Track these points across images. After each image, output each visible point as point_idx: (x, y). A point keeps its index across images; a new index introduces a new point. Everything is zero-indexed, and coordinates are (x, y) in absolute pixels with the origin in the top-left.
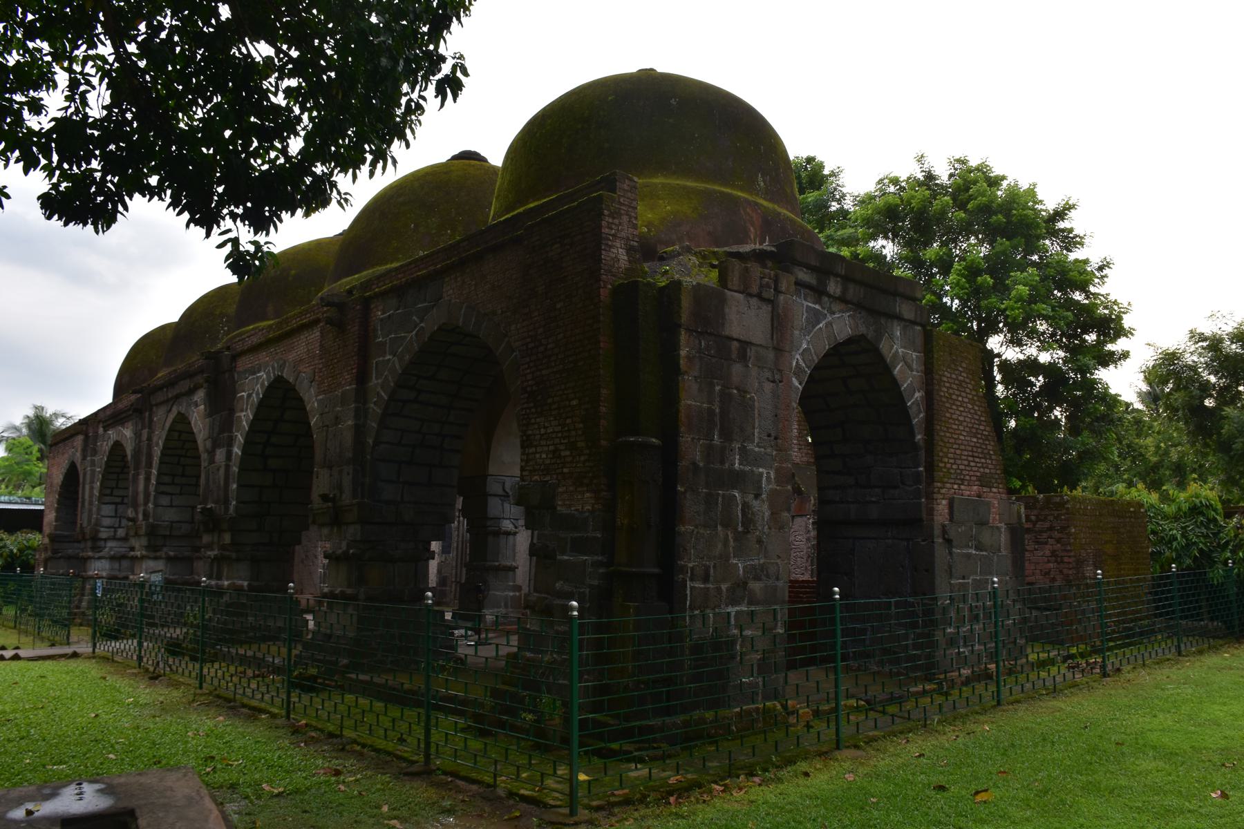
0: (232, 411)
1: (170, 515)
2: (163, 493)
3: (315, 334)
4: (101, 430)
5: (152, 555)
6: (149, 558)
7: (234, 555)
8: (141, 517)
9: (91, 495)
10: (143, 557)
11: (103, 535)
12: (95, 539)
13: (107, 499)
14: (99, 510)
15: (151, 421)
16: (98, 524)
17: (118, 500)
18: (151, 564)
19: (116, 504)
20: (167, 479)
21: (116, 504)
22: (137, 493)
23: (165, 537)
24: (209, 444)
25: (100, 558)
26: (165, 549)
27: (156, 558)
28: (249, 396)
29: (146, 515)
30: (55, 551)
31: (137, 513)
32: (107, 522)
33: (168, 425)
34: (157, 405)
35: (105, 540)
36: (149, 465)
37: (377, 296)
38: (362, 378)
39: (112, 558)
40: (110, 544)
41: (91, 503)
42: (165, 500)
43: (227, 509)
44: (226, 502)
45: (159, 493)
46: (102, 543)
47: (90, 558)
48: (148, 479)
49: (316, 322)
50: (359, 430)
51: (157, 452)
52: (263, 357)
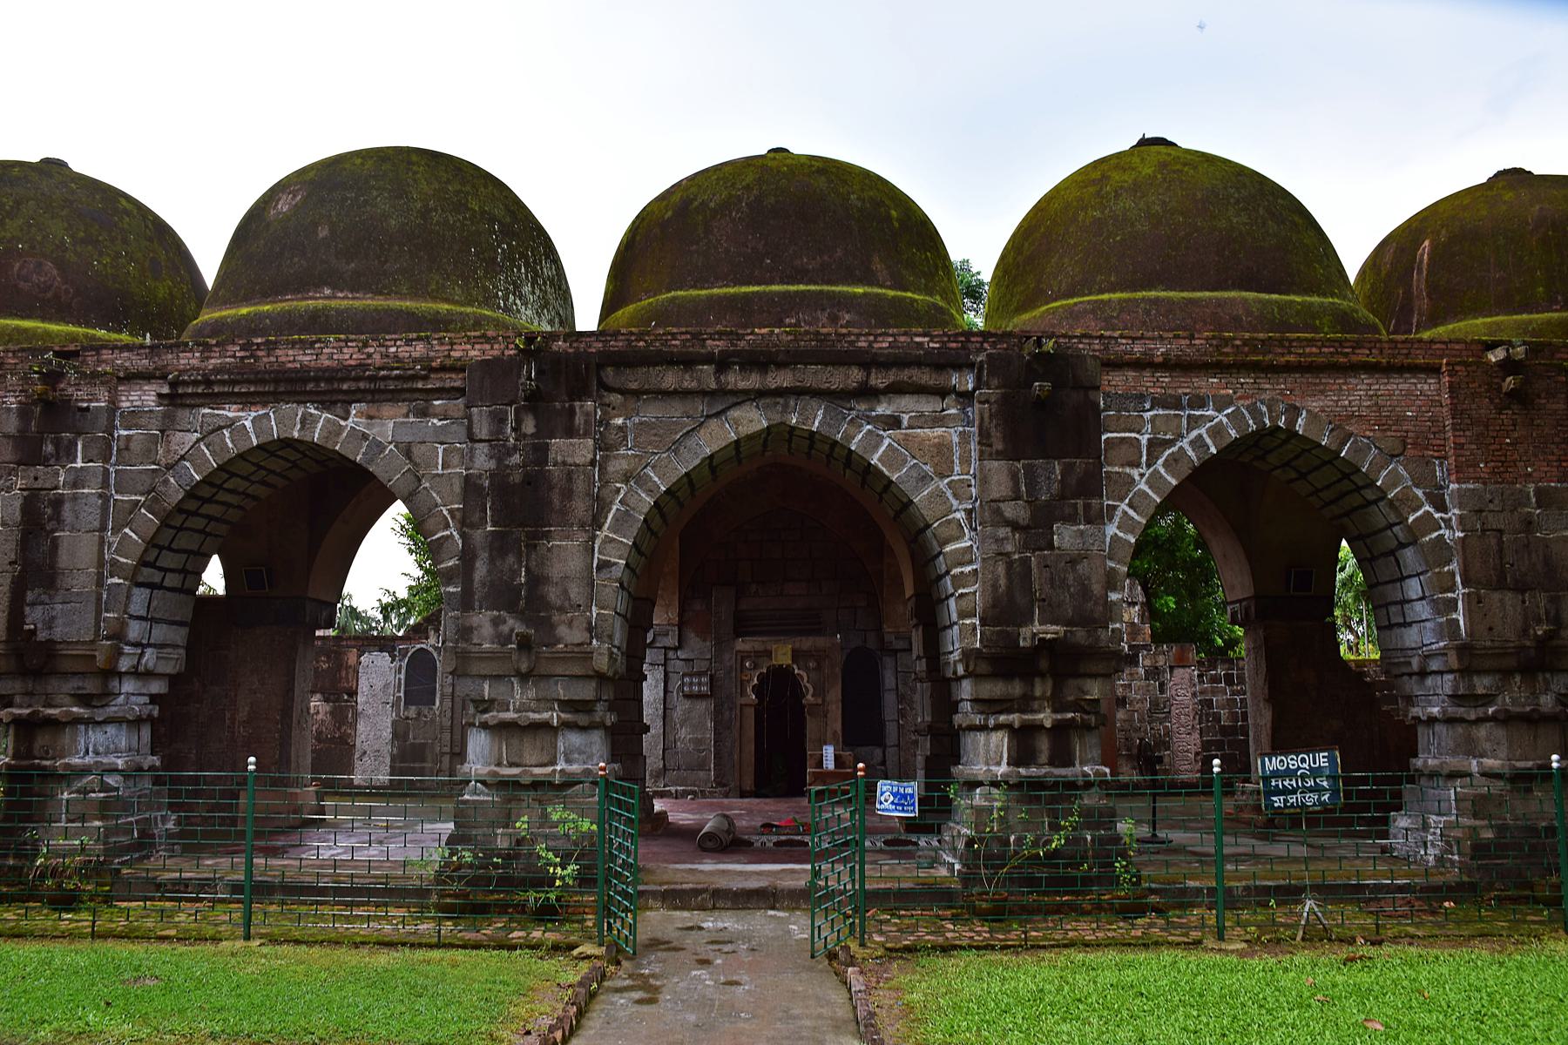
3: (1428, 386)
4: (145, 397)
5: (582, 719)
10: (566, 725)
13: (147, 574)
16: (118, 636)
18: (575, 739)
25: (106, 722)
28: (1156, 446)
47: (77, 721)
49: (1434, 370)
52: (1210, 384)
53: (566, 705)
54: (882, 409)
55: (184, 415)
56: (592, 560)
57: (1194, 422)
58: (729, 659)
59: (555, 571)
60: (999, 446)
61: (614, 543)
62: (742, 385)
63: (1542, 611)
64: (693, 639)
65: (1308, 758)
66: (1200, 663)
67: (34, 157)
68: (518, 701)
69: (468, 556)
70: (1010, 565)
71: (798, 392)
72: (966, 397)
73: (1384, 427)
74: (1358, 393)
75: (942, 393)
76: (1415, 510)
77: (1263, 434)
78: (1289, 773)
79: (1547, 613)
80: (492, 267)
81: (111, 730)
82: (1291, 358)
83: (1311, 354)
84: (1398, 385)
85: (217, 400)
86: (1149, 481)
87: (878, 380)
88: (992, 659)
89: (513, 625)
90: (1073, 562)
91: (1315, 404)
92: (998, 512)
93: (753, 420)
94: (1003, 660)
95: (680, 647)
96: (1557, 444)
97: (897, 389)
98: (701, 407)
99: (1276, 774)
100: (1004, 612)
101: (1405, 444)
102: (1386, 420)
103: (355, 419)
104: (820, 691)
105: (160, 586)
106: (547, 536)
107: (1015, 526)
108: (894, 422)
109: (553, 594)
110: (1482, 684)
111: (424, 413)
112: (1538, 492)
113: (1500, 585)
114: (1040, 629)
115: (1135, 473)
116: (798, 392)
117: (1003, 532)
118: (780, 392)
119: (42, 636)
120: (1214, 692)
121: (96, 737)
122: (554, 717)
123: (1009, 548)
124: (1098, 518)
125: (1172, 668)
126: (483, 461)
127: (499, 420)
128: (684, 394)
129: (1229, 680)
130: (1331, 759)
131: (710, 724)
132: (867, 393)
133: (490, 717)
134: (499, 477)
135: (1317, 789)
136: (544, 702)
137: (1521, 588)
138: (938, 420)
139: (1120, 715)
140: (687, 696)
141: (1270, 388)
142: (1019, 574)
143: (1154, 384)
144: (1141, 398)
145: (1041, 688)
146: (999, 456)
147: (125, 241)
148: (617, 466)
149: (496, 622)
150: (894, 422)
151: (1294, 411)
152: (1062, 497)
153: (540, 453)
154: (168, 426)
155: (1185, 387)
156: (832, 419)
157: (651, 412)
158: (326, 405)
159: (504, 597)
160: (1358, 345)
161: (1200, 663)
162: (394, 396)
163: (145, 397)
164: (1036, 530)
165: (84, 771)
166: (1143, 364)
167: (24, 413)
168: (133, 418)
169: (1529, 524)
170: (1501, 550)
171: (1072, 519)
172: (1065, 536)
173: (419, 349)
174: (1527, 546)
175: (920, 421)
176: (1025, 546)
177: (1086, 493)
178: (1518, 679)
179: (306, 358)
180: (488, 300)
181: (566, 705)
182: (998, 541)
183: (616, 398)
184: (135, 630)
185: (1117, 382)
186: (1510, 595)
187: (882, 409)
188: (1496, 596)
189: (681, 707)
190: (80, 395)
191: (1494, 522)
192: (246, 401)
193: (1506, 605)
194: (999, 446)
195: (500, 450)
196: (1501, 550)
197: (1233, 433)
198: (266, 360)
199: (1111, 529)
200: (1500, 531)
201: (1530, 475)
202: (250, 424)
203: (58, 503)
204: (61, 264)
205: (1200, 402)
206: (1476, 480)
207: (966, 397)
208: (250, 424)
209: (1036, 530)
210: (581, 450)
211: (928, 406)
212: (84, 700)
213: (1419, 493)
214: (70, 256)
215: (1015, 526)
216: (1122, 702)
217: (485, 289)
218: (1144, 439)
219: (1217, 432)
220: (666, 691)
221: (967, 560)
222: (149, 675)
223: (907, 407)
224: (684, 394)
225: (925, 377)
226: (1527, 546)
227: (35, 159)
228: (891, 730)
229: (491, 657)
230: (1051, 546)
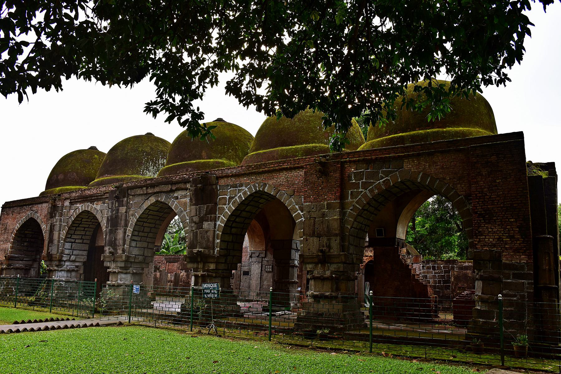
0: (216, 204)
1: (135, 252)
2: (134, 240)
4: (67, 203)
5: (125, 271)
6: (122, 273)
7: (214, 275)
8: (120, 252)
9: (59, 237)
10: (119, 272)
11: (64, 259)
12: (60, 260)
13: (68, 240)
14: (64, 245)
15: (128, 203)
16: (62, 253)
17: (73, 241)
18: (123, 276)
19: (72, 242)
20: (136, 233)
21: (72, 242)
22: (116, 239)
23: (131, 262)
24: (196, 219)
25: (61, 271)
26: (131, 269)
27: (126, 273)
28: (231, 198)
29: (124, 251)
30: (9, 265)
31: (116, 249)
32: (67, 252)
33: (145, 206)
34: (133, 196)
35: (65, 261)
36: (126, 225)
37: (350, 162)
38: (342, 197)
39: (68, 271)
40: (67, 263)
41: (59, 241)
42: (134, 244)
43: (214, 252)
44: (214, 249)
45: (132, 240)
46: (63, 263)
47: (55, 270)
48: (125, 233)
49: (302, 167)
50: (342, 221)
51: (133, 221)
52: (244, 180)
53: (121, 268)
54: (176, 195)
57: (240, 191)
59: (118, 238)
60: (194, 202)
62: (150, 192)
63: (325, 244)
64: (268, 253)
65: (213, 285)
66: (423, 262)
67: (86, 147)
70: (193, 233)
71: (161, 192)
73: (289, 187)
74: (282, 178)
76: (295, 212)
77: (256, 192)
78: (208, 288)
79: (326, 244)
80: (141, 164)
81: (63, 272)
82: (266, 169)
83: (272, 167)
84: (294, 173)
86: (228, 209)
88: (189, 257)
89: (111, 250)
91: (271, 182)
92: (192, 220)
93: (153, 200)
95: (265, 257)
96: (335, 188)
97: (178, 190)
98: (144, 197)
99: (206, 289)
101: (294, 192)
102: (290, 184)
105: (75, 242)
106: (117, 229)
107: (195, 223)
109: (117, 243)
110: (309, 267)
111: (104, 203)
112: (327, 204)
113: (313, 235)
115: (225, 207)
116: (161, 192)
117: (193, 224)
118: (157, 193)
120: (428, 273)
121: (60, 274)
123: (194, 229)
125: (412, 264)
126: (110, 214)
128: (142, 195)
129: (434, 268)
130: (218, 285)
132: (172, 191)
134: (111, 216)
135: (214, 293)
136: (117, 267)
137: (319, 236)
140: (266, 272)
141: (260, 178)
142: (195, 235)
143: (230, 181)
144: (228, 185)
145: (201, 266)
146: (195, 205)
147: (92, 165)
148: (131, 212)
149: (109, 249)
150: (177, 198)
151: (265, 185)
152: (206, 215)
155: (237, 181)
156: (167, 198)
157: (137, 200)
158: (91, 203)
160: (284, 162)
161: (423, 262)
164: (199, 225)
165: (56, 281)
166: (227, 176)
169: (324, 215)
170: (314, 224)
171: (207, 221)
172: (206, 225)
173: (104, 188)
174: (322, 222)
176: (197, 228)
177: (211, 214)
178: (320, 265)
180: (138, 173)
181: (121, 268)
182: (192, 227)
183: (131, 197)
184: (67, 252)
185: (222, 182)
186: (315, 238)
187: (176, 195)
188: (312, 238)
189: (265, 275)
191: (313, 215)
192: (80, 202)
193: (314, 242)
194: (194, 202)
196: (314, 224)
197: (248, 193)
200: (315, 218)
201: (326, 199)
202: (81, 207)
204: (77, 173)
205: (241, 185)
206: (310, 202)
208: (81, 207)
209: (199, 225)
212: (57, 266)
213: (297, 207)
214: (79, 171)
215: (195, 223)
217: (137, 170)
218: (228, 197)
219: (245, 193)
220: (261, 270)
222: (74, 261)
224: (142, 195)
225: (182, 186)
226: (322, 222)
227: (87, 148)
229: (109, 257)
230: (202, 228)
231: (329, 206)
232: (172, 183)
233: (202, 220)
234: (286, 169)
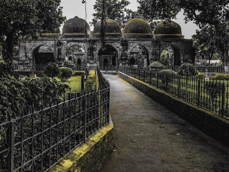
4: (65, 42)
54: (114, 43)
55: (68, 43)
56: (96, 53)
58: (101, 57)
61: (97, 52)
68: (91, 61)
69: (88, 53)
72: (120, 43)
75: (118, 42)
84: (148, 42)
85: (71, 42)
87: (114, 42)
90: (126, 53)
94: (121, 59)
100: (122, 56)
103: (80, 44)
104: (110, 60)
108: (115, 44)
114: (124, 57)
119: (60, 58)
122: (94, 62)
124: (127, 50)
127: (90, 44)
131: (99, 63)
133: (90, 63)
136: (93, 62)
138: (118, 44)
139: (139, 63)
142: (122, 54)
148: (97, 47)
150: (115, 44)
151: (141, 43)
153: (92, 46)
154: (67, 44)
159: (90, 55)
162: (83, 42)
163: (65, 42)
167: (58, 43)
168: (65, 43)
169: (156, 51)
172: (125, 52)
175: (117, 44)
176: (123, 52)
179: (76, 39)
185: (129, 42)
187: (114, 43)
190: (61, 42)
192: (73, 42)
193: (154, 56)
195: (90, 46)
198: (74, 39)
199: (129, 51)
203: (60, 49)
205: (135, 43)
207: (120, 43)
209: (124, 52)
210: (95, 46)
211: (117, 43)
212: (63, 62)
216: (139, 62)
221: (120, 53)
223: (116, 43)
228: (117, 64)
231: (157, 49)
232: (113, 40)
233: (124, 50)
234: (147, 41)
